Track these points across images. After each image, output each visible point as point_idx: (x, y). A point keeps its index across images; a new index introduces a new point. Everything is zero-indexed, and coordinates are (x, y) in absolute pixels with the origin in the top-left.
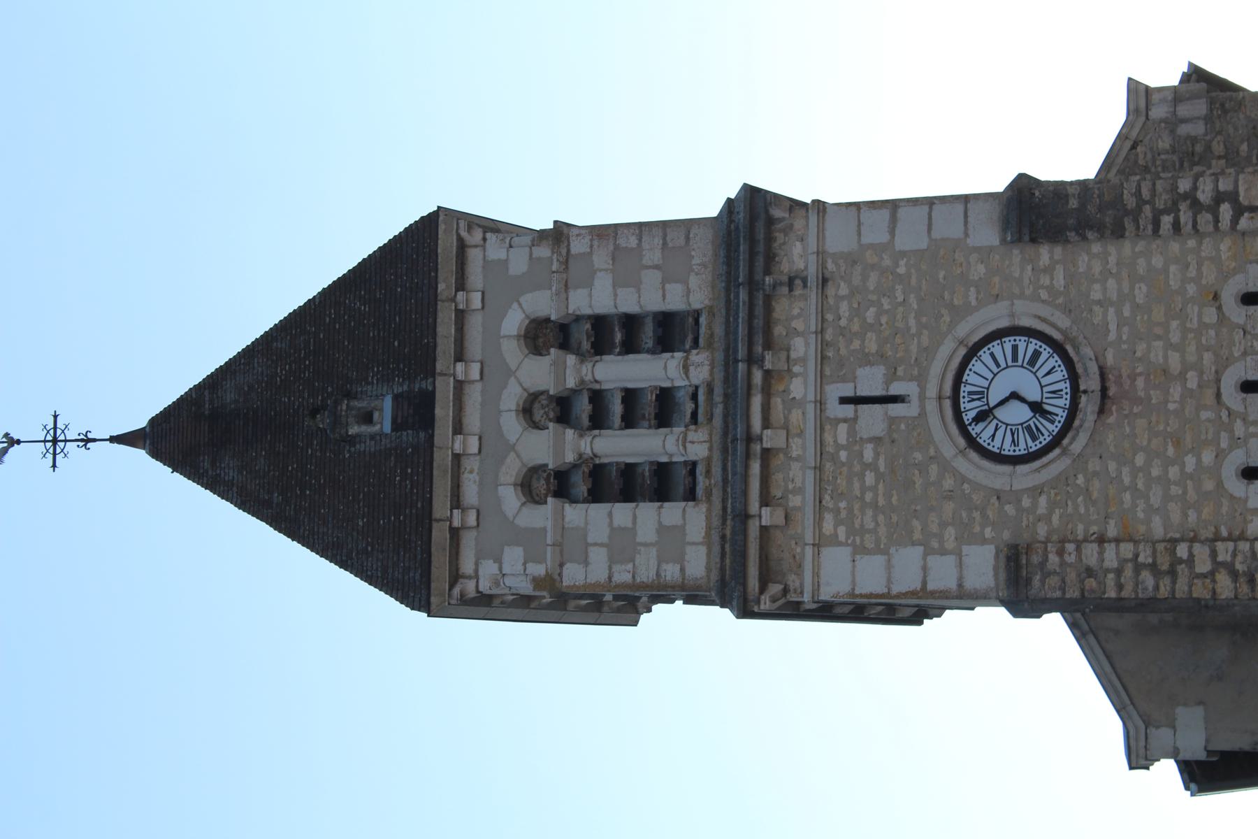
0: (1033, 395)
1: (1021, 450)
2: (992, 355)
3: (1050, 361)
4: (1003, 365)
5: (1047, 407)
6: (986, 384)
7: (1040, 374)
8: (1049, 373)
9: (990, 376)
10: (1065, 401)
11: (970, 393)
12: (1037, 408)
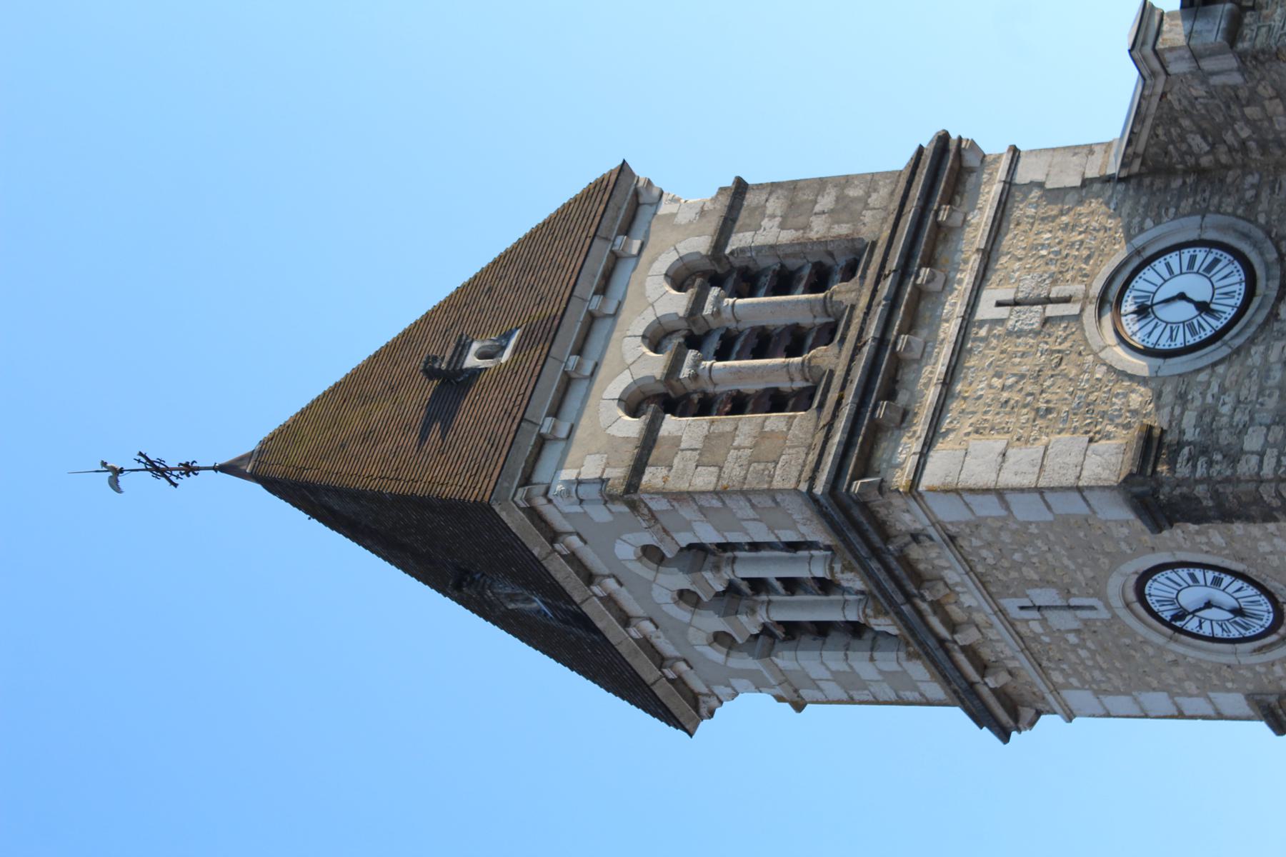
1: (1179, 343)
4: (1176, 270)
5: (1213, 306)
6: (1153, 289)
9: (1159, 281)
10: (1237, 301)
12: (1203, 307)
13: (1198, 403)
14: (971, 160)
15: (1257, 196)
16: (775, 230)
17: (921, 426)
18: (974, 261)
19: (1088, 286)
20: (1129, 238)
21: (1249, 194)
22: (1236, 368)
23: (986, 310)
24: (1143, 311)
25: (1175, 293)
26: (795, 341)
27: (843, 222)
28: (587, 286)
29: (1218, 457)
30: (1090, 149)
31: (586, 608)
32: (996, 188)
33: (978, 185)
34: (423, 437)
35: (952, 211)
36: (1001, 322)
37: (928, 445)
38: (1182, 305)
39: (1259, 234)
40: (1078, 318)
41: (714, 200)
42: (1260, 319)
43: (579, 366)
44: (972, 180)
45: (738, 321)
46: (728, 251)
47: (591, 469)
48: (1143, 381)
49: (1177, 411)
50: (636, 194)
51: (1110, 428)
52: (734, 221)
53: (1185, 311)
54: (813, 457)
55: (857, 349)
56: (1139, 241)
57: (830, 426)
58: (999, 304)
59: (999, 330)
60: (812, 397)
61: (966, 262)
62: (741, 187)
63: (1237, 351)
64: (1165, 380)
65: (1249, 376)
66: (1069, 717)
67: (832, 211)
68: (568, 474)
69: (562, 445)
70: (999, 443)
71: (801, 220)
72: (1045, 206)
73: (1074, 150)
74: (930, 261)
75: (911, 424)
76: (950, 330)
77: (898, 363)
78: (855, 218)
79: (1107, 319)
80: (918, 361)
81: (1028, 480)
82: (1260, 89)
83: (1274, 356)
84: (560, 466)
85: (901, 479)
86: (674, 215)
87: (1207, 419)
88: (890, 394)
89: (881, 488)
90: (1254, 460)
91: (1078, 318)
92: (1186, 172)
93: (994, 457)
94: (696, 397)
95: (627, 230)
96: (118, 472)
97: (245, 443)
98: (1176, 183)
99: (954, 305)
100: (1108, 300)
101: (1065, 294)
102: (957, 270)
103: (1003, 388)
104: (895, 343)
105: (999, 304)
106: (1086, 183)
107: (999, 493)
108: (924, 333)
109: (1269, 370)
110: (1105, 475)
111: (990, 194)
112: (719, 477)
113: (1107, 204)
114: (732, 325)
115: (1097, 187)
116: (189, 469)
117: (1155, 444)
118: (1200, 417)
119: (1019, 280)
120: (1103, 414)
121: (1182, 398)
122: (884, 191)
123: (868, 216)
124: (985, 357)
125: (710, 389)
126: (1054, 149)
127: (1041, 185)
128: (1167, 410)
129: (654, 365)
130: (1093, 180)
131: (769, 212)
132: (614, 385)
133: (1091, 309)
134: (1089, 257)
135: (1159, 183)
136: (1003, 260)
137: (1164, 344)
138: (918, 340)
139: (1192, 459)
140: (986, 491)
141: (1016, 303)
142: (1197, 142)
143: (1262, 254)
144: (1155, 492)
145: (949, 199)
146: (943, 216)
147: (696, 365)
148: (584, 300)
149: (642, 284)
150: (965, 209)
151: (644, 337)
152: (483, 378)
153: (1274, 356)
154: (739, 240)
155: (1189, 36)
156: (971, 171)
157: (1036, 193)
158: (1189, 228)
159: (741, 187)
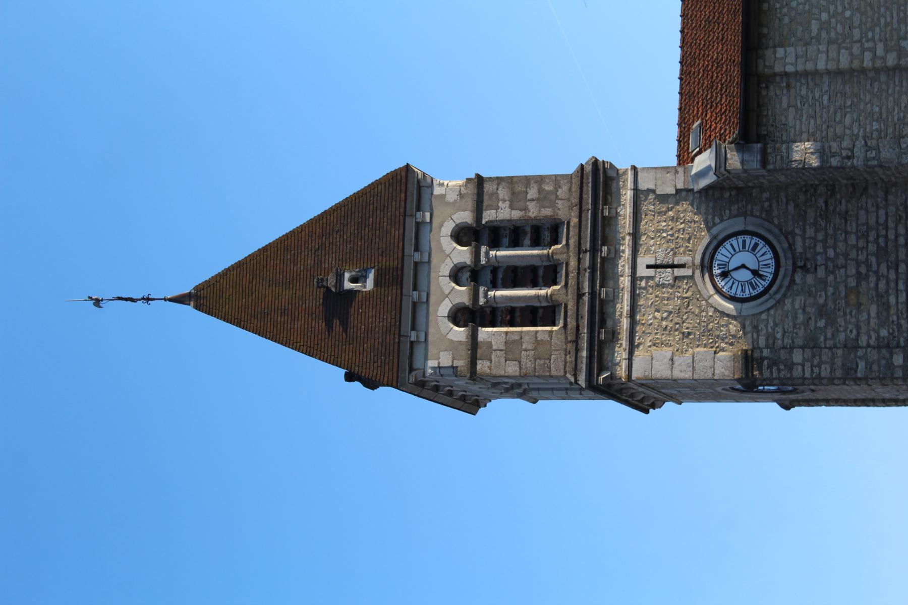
0: (753, 265)
1: (747, 294)
2: (732, 245)
3: (763, 248)
4: (737, 250)
5: (760, 272)
6: (727, 260)
7: (758, 255)
8: (763, 255)
9: (730, 256)
10: (772, 270)
11: (718, 265)
12: (755, 273)
13: (764, 332)
14: (612, 173)
15: (770, 206)
16: (508, 209)
19: (693, 258)
20: (709, 229)
21: (766, 204)
22: (779, 312)
23: (642, 271)
24: (725, 275)
25: (740, 265)
27: (546, 207)
28: (409, 248)
29: (782, 367)
34: (329, 327)
35: (610, 209)
36: (652, 278)
37: (631, 353)
39: (776, 231)
40: (691, 277)
42: (786, 283)
43: (419, 296)
44: (614, 185)
45: (498, 262)
46: (484, 222)
47: (446, 360)
48: (734, 318)
49: (755, 336)
50: (418, 181)
51: (723, 345)
53: (745, 275)
55: (580, 296)
56: (715, 231)
57: (576, 341)
58: (648, 267)
59: (651, 283)
60: (554, 312)
61: (624, 239)
62: (480, 181)
63: (778, 302)
64: (745, 318)
65: (787, 316)
67: (538, 200)
68: (432, 363)
69: (422, 346)
70: (667, 352)
71: (521, 204)
72: (659, 204)
75: (618, 340)
77: (603, 302)
78: (553, 205)
79: (707, 276)
80: (613, 301)
83: (797, 306)
85: (622, 372)
87: (771, 341)
88: (603, 323)
89: (612, 376)
90: (800, 368)
91: (691, 277)
92: (730, 189)
93: (667, 360)
94: (488, 310)
98: (727, 195)
99: (623, 266)
100: (706, 266)
101: (682, 262)
102: (620, 244)
103: (662, 319)
104: (600, 294)
105: (648, 267)
106: (678, 191)
108: (611, 283)
109: (796, 313)
110: (727, 373)
111: (627, 195)
112: (520, 368)
113: (692, 205)
114: (496, 265)
115: (684, 194)
116: (147, 299)
117: (750, 359)
118: (767, 340)
120: (718, 336)
121: (756, 328)
122: (565, 188)
123: (560, 203)
124: (647, 299)
125: (495, 305)
126: (656, 168)
127: (654, 191)
128: (750, 335)
131: (501, 197)
133: (698, 273)
134: (689, 239)
136: (643, 238)
137: (739, 294)
139: (770, 367)
143: (780, 243)
145: (605, 203)
146: (606, 213)
147: (486, 295)
148: (410, 256)
149: (439, 242)
150: (614, 205)
151: (450, 276)
153: (797, 306)
154: (489, 216)
155: (742, 162)
156: (612, 179)
157: (651, 196)
158: (738, 224)
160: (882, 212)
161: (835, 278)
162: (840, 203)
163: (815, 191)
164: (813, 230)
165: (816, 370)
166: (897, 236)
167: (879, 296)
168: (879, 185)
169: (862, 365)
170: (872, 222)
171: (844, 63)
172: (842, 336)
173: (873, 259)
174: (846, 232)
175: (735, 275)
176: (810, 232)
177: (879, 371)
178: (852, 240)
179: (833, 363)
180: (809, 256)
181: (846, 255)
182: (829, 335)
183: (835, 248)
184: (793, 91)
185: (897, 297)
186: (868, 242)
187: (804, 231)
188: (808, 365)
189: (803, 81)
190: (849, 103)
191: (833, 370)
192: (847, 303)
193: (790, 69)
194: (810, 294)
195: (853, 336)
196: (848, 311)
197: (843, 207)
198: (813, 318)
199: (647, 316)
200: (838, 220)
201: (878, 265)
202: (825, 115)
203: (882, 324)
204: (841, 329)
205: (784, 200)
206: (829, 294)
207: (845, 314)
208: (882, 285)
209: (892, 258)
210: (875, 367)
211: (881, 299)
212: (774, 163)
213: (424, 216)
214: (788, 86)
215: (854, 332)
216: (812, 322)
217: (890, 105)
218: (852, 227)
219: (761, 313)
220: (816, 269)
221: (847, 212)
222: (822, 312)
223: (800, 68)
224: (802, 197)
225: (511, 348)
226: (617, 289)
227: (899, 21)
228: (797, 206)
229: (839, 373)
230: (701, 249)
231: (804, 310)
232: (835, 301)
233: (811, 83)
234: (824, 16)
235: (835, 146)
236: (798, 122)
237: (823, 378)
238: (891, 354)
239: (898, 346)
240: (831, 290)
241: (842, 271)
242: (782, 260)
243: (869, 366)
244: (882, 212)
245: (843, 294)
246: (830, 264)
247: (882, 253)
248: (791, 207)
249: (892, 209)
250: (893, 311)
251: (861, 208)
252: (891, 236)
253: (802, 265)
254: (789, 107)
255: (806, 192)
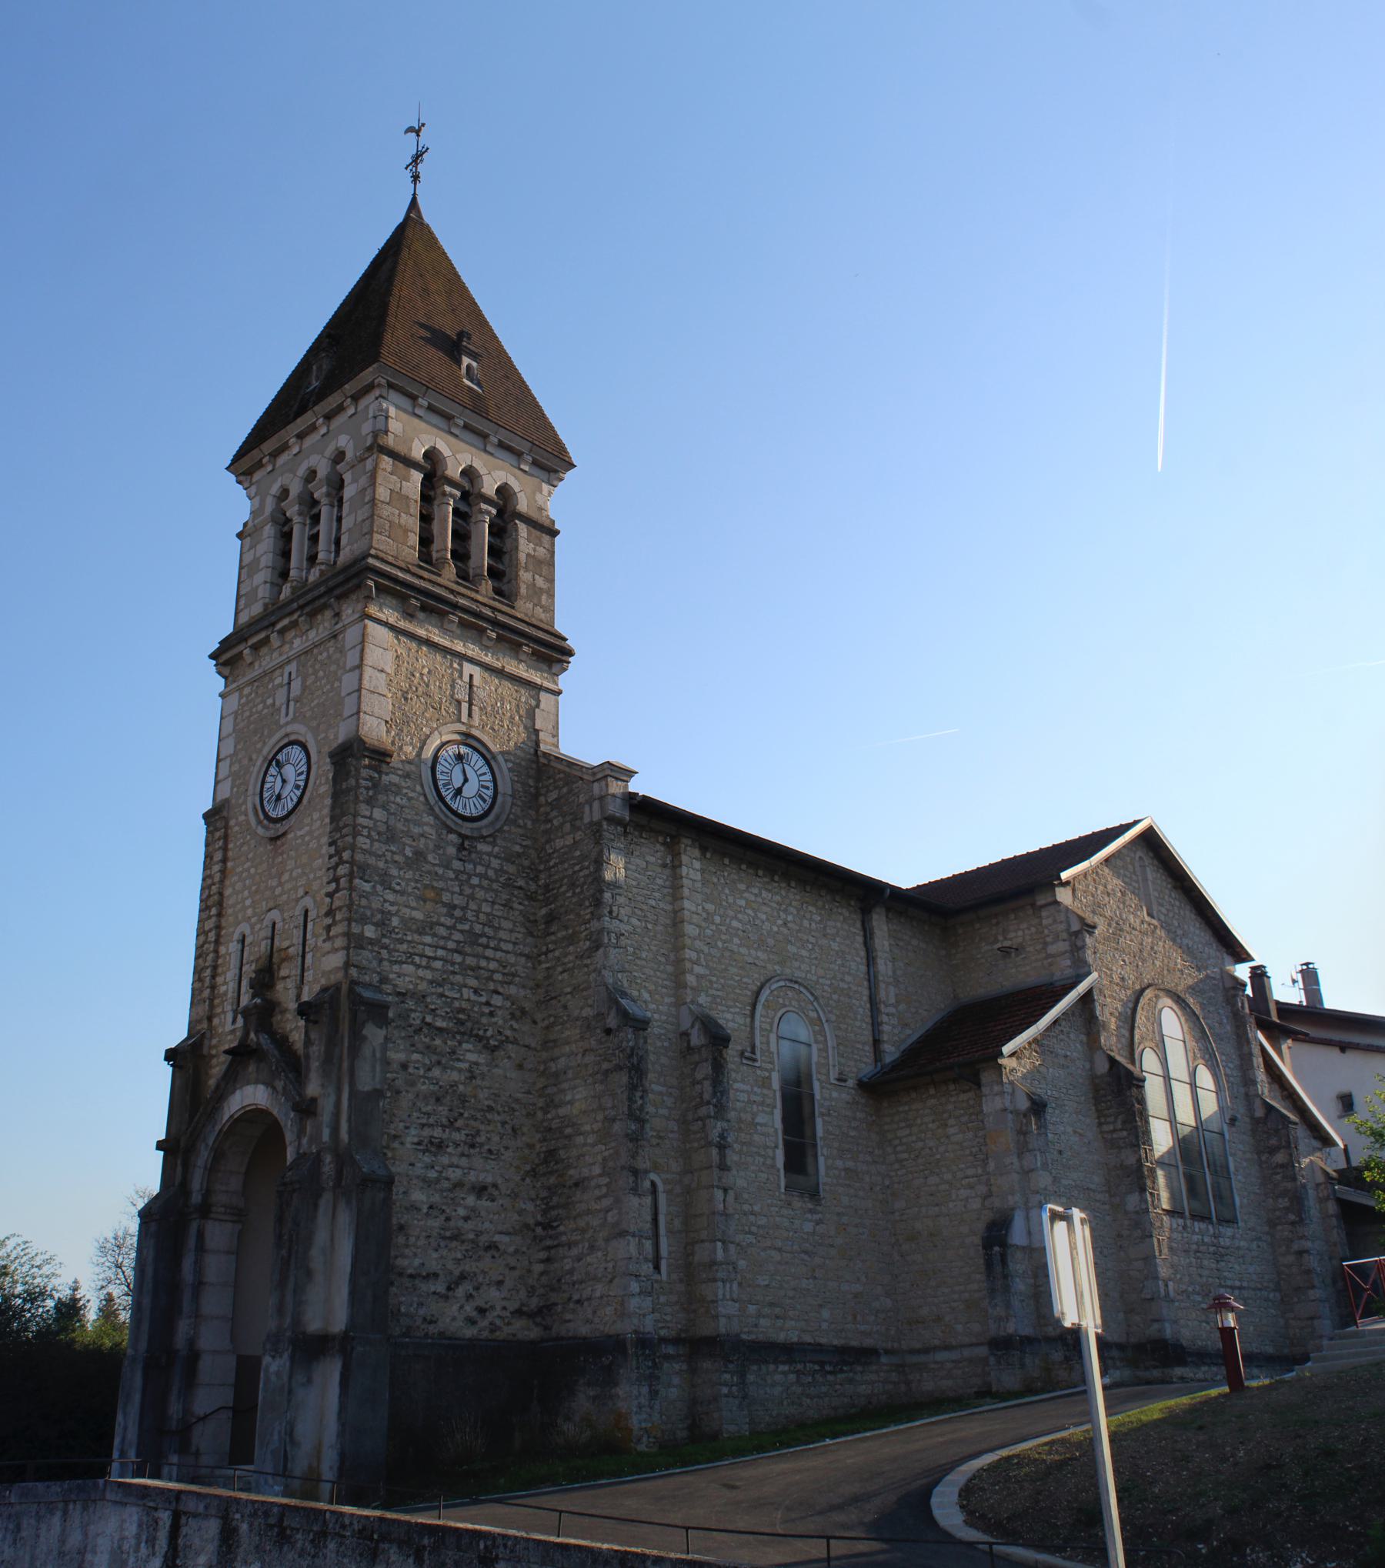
1: (439, 776)
4: (481, 778)
9: (476, 768)
10: (461, 811)
12: (459, 791)
13: (403, 784)
14: (556, 668)
15: (520, 826)
16: (527, 551)
17: (403, 624)
18: (498, 664)
20: (502, 753)
21: (521, 822)
22: (422, 807)
23: (468, 668)
24: (459, 758)
26: (460, 556)
29: (371, 793)
30: (556, 735)
31: (310, 413)
32: (538, 681)
33: (541, 670)
34: (422, 326)
35: (528, 654)
36: (461, 677)
38: (461, 781)
39: (498, 826)
40: (459, 720)
41: (548, 517)
42: (449, 822)
43: (457, 426)
44: (545, 667)
45: (475, 523)
47: (394, 426)
48: (419, 754)
49: (400, 772)
50: (556, 471)
51: (393, 733)
52: (534, 527)
53: (457, 781)
54: (390, 559)
55: (452, 591)
56: (500, 758)
57: (408, 571)
58: (471, 676)
59: (456, 675)
61: (498, 659)
62: (553, 533)
63: (432, 809)
64: (418, 767)
65: (416, 814)
66: (222, 695)
67: (534, 585)
68: (392, 411)
69: (410, 409)
70: (390, 669)
71: (531, 567)
73: (556, 727)
74: (500, 638)
75: (405, 619)
76: (459, 647)
77: (442, 614)
78: (529, 598)
79: (457, 737)
80: (442, 627)
81: (366, 683)
82: (580, 833)
83: (427, 829)
84: (397, 407)
85: (373, 610)
86: (541, 492)
88: (424, 608)
89: (369, 598)
90: (368, 813)
91: (459, 720)
92: (537, 788)
94: (432, 493)
95: (535, 463)
96: (418, 132)
97: (428, 216)
98: (531, 782)
99: (473, 650)
100: (467, 738)
101: (474, 715)
102: (493, 654)
103: (421, 674)
104: (453, 614)
105: (471, 676)
106: (537, 732)
107: (360, 667)
108: (458, 632)
109: (419, 825)
110: (366, 728)
111: (536, 677)
112: (383, 502)
113: (523, 743)
114: (473, 520)
116: (416, 178)
118: (395, 785)
119: (484, 689)
120: (401, 730)
121: (407, 776)
122: (543, 616)
124: (441, 665)
125: (436, 502)
127: (538, 706)
128: (401, 766)
129: (454, 471)
130: (537, 735)
132: (443, 446)
133: (463, 728)
134: (494, 730)
135: (532, 772)
136: (496, 681)
137: (439, 768)
138: (454, 627)
139: (371, 778)
140: (362, 659)
141: (471, 686)
142: (553, 795)
143: (486, 826)
144: (352, 756)
145: (535, 653)
147: (452, 496)
149: (502, 469)
151: (471, 466)
152: (455, 367)
153: (427, 829)
154: (523, 529)
155: (614, 796)
156: (550, 667)
157: (533, 703)
158: (505, 787)
159: (553, 533)
160: (510, 947)
161: (451, 880)
162: (520, 904)
163: (532, 879)
164: (497, 867)
165: (365, 832)
166: (487, 959)
167: (432, 925)
168: (535, 951)
169: (367, 887)
170: (502, 934)
171: (690, 930)
172: (394, 872)
173: (466, 927)
174: (493, 903)
175: (458, 769)
176: (495, 863)
177: (359, 906)
178: (486, 908)
179: (370, 853)
180: (473, 856)
181: (472, 897)
182: (397, 858)
183: (480, 886)
184: (659, 870)
185: (429, 945)
186: (484, 925)
187: (496, 857)
188: (370, 823)
189: (667, 883)
190: (650, 926)
191: (364, 851)
192: (426, 887)
193: (684, 870)
194: (437, 847)
195: (394, 885)
196: (419, 885)
197: (516, 906)
198: (414, 844)
199: (426, 660)
200: (505, 897)
201: (462, 932)
202: (639, 898)
203: (404, 921)
204: (402, 873)
205: (524, 843)
206: (437, 868)
207: (417, 881)
208: (442, 931)
209: (468, 949)
210: (364, 902)
211: (422, 929)
212: (608, 831)
213: (526, 463)
214: (664, 866)
215: (398, 888)
216: (408, 841)
217: (647, 971)
218: (498, 910)
219: (422, 786)
220: (461, 860)
221: (511, 908)
222: (419, 855)
223: (685, 881)
224: (526, 863)
225: (398, 498)
226: (453, 636)
227: (714, 997)
228: (519, 855)
229: (359, 857)
230: (485, 739)
231: (422, 835)
232: (429, 872)
233: (666, 891)
234: (717, 919)
235: (621, 900)
236: (634, 868)
237: (354, 838)
238: (376, 925)
239: (384, 936)
240: (440, 871)
241: (457, 889)
242: (485, 821)
243: (364, 895)
244: (510, 947)
245: (435, 884)
246: (465, 877)
247: (473, 938)
248: (517, 848)
249: (512, 959)
250: (416, 937)
251: (514, 925)
252: (489, 953)
253: (465, 846)
254: (647, 862)
255: (529, 868)
